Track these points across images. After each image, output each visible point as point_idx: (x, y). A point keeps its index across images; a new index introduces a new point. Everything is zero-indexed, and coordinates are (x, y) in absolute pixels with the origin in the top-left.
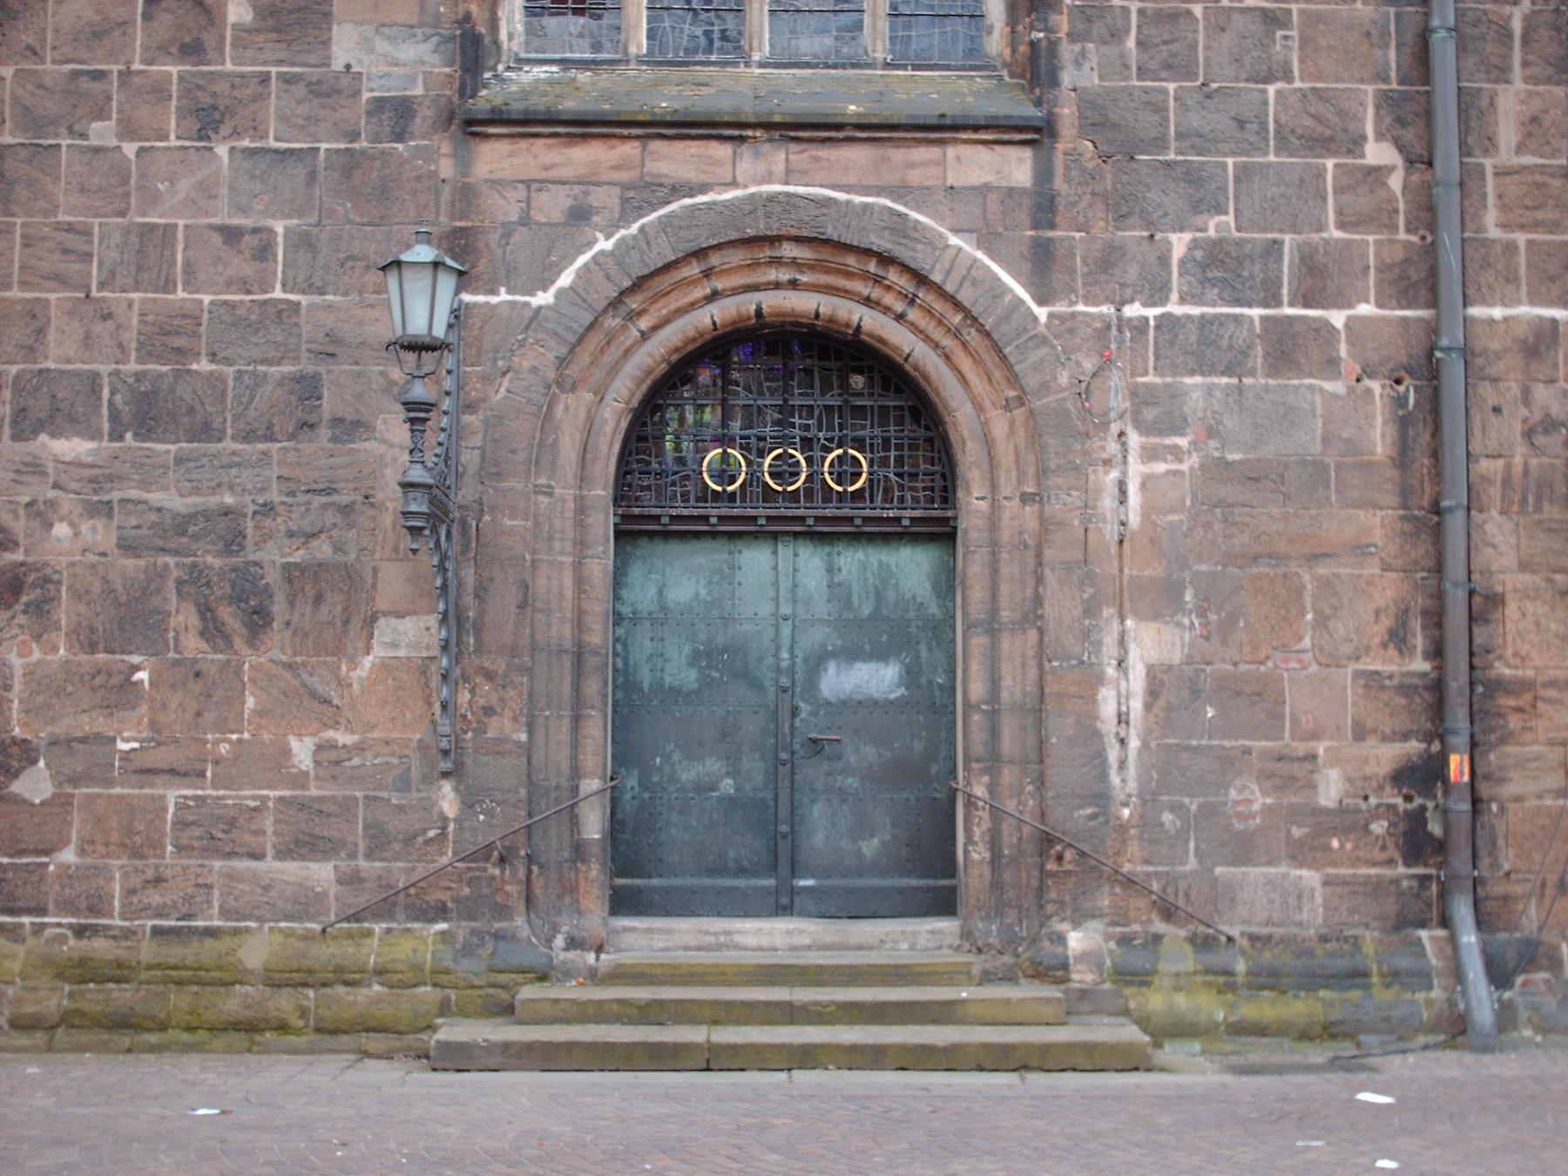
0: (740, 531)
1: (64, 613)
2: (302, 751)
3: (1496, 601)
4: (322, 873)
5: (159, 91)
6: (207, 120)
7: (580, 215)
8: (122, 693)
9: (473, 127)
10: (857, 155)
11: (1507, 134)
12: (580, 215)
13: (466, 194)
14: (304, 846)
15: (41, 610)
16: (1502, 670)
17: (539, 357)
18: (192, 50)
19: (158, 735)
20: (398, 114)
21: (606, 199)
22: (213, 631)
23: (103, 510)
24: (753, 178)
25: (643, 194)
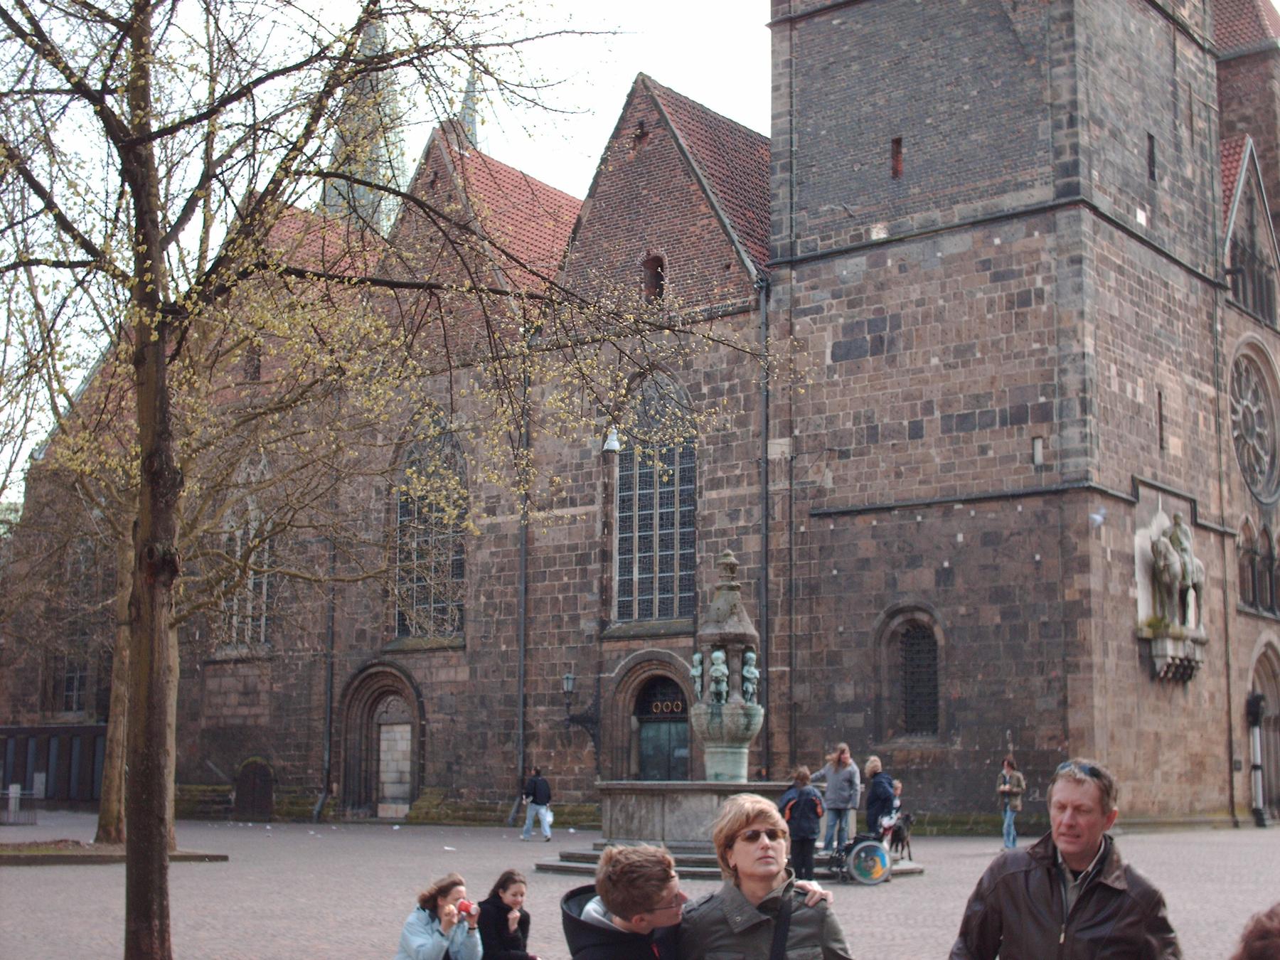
0: (664, 720)
1: (541, 741)
2: (576, 769)
3: (773, 734)
4: (579, 793)
5: (554, 635)
6: (562, 640)
7: (619, 657)
8: (549, 757)
9: (601, 639)
10: (664, 641)
11: (777, 628)
12: (619, 657)
13: (601, 654)
14: (577, 788)
15: (537, 741)
16: (774, 750)
17: (612, 687)
18: (559, 627)
19: (555, 766)
20: (590, 637)
21: (623, 653)
22: (563, 745)
23: (546, 721)
24: (646, 647)
25: (629, 651)
